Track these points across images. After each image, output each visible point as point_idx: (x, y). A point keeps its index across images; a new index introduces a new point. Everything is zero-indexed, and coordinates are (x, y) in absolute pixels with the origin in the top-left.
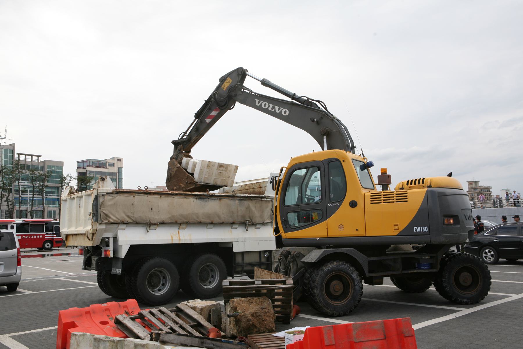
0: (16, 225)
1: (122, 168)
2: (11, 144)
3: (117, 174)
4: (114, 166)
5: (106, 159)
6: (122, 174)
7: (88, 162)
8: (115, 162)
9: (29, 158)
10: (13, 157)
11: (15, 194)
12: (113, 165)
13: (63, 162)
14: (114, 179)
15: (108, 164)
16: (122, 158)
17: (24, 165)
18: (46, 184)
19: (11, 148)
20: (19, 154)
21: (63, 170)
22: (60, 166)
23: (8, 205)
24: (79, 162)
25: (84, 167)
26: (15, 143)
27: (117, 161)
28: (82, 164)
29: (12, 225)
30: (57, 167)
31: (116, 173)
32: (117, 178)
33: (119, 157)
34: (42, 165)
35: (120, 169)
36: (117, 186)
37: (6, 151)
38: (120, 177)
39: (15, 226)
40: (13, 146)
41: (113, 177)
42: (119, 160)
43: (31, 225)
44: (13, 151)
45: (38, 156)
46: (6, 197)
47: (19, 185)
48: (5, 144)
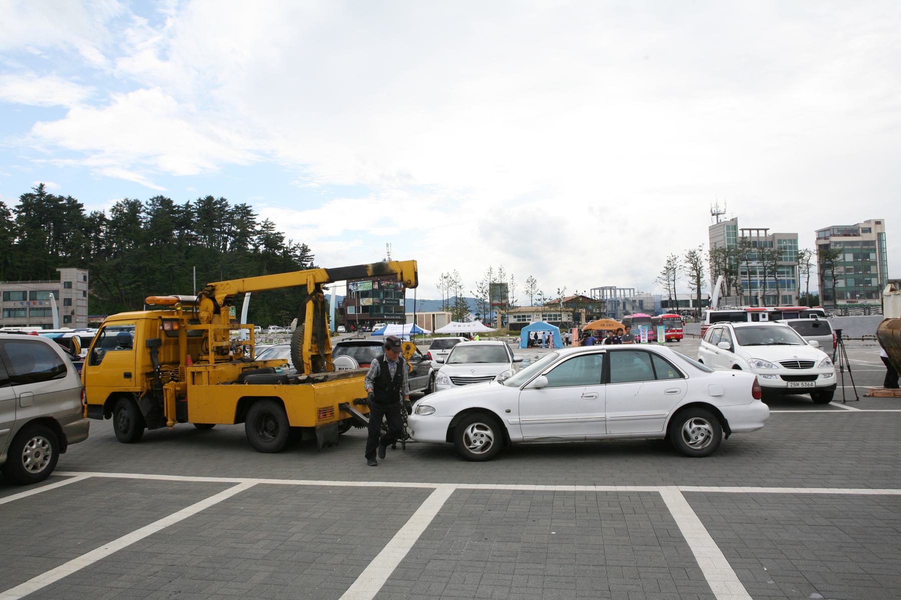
0: (767, 313)
1: (884, 234)
2: (733, 219)
3: (877, 242)
4: (871, 232)
5: (858, 224)
6: (884, 242)
7: (832, 230)
8: (872, 226)
9: (754, 233)
10: (736, 234)
11: (742, 277)
12: (869, 230)
13: (797, 234)
14: (871, 250)
15: (860, 229)
16: (883, 220)
17: (749, 242)
18: (779, 263)
19: (733, 223)
20: (743, 230)
21: (797, 243)
22: (793, 239)
23: (737, 291)
24: (819, 232)
25: (825, 237)
26: (737, 218)
27: (876, 224)
28: (824, 234)
29: (764, 313)
30: (790, 241)
31: (875, 241)
32: (877, 247)
33: (878, 218)
34: (770, 240)
35: (880, 235)
36: (878, 259)
37: (728, 227)
38: (881, 246)
39: (767, 315)
40: (735, 220)
41: (871, 247)
42: (878, 223)
43: (784, 313)
44: (735, 227)
45: (766, 230)
46: (734, 281)
47: (748, 267)
48: (726, 220)
